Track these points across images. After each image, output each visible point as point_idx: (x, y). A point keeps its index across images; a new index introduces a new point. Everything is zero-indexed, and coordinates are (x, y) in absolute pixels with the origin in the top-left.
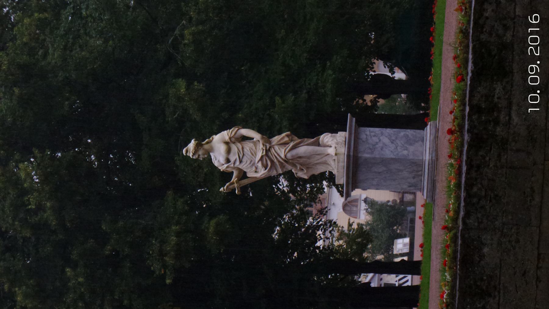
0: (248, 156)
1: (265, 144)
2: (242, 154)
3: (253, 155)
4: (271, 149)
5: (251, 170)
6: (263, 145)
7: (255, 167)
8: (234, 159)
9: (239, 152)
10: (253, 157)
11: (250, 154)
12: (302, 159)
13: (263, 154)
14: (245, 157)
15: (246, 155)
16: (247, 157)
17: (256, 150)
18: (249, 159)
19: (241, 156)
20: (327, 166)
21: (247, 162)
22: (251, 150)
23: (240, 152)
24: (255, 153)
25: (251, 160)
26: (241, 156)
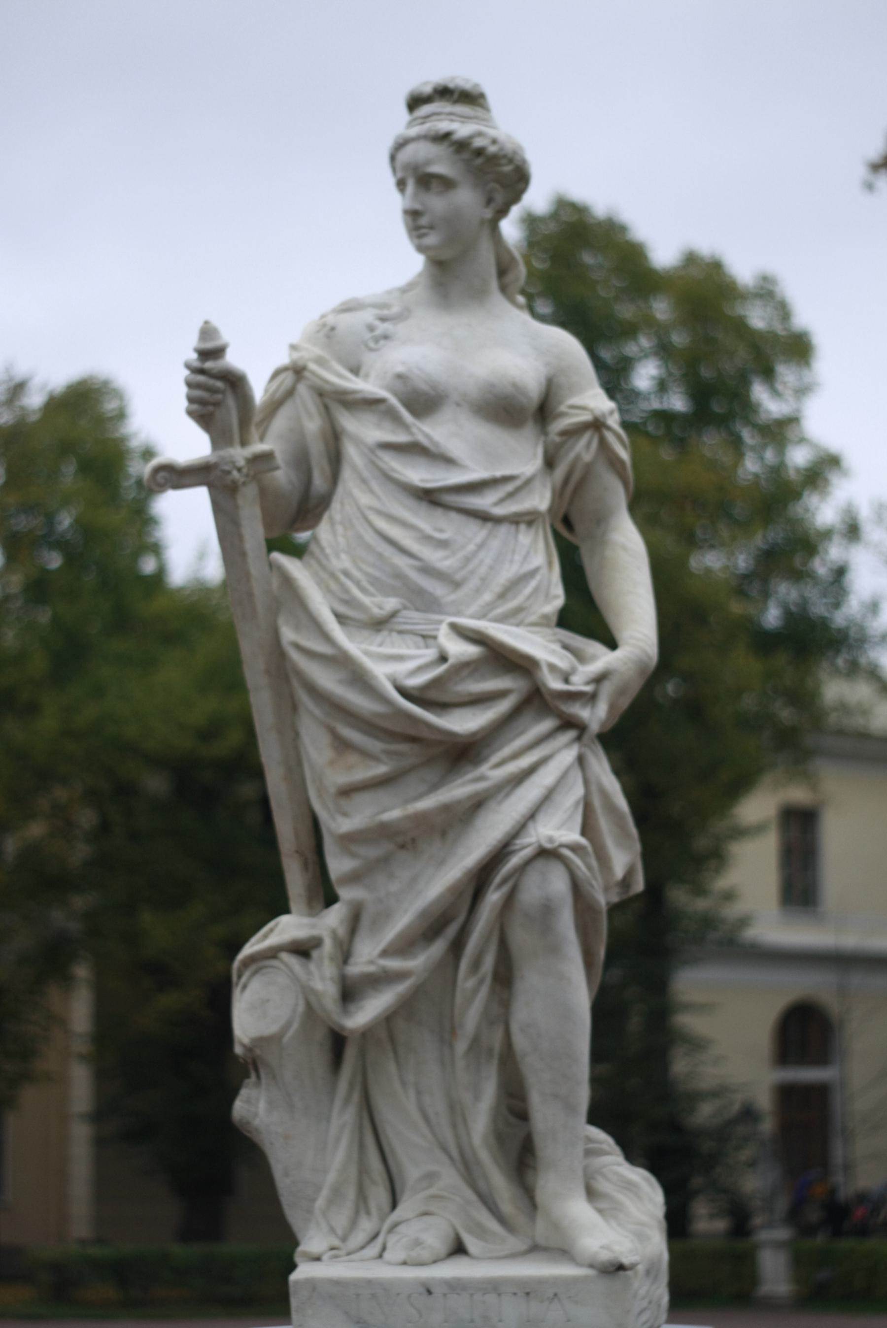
0: (487, 557)
1: (607, 689)
2: (499, 511)
3: (503, 595)
4: (571, 734)
5: (358, 584)
6: (600, 679)
7: (394, 614)
8: (454, 447)
9: (510, 487)
10: (487, 597)
11: (508, 572)
12: (484, 991)
13: (545, 670)
14: (475, 532)
15: (495, 544)
16: (481, 546)
17: (533, 618)
18: (468, 560)
19: (485, 501)
20: (351, 1193)
21: (443, 544)
22: (533, 583)
23: (511, 495)
24: (519, 610)
25: (458, 577)
26: (485, 501)
